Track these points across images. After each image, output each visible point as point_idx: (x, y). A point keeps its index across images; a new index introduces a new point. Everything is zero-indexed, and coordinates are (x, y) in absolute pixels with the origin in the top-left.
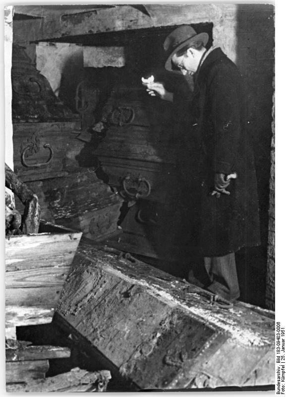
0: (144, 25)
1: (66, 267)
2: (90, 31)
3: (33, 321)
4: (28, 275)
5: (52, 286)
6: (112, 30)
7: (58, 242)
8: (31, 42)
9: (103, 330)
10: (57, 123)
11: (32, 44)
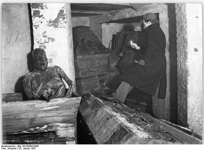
0: (136, 15)
1: (77, 109)
2: (118, 19)
3: (66, 128)
4: (62, 112)
5: (72, 116)
6: (125, 18)
7: (72, 100)
8: (100, 24)
9: (98, 132)
10: (102, 54)
11: (100, 24)
